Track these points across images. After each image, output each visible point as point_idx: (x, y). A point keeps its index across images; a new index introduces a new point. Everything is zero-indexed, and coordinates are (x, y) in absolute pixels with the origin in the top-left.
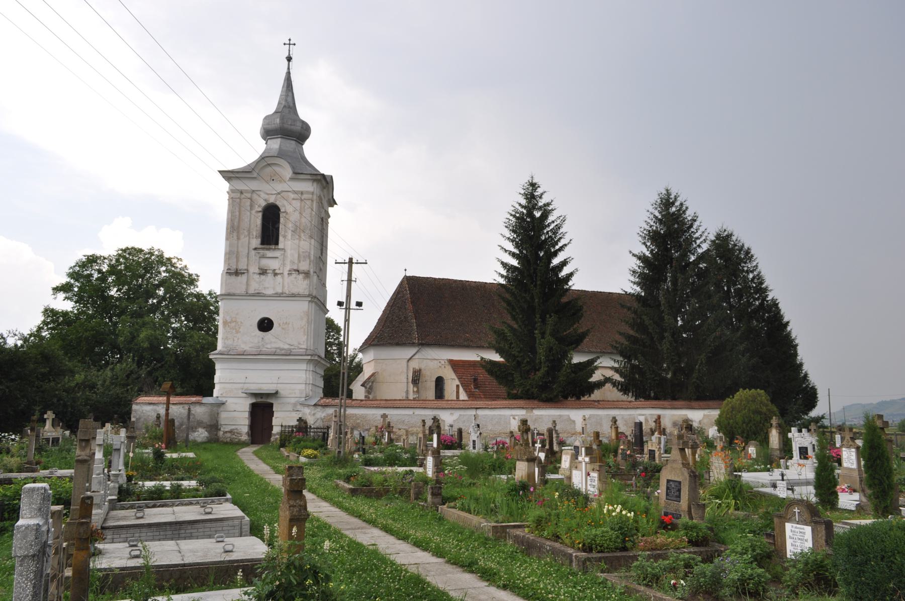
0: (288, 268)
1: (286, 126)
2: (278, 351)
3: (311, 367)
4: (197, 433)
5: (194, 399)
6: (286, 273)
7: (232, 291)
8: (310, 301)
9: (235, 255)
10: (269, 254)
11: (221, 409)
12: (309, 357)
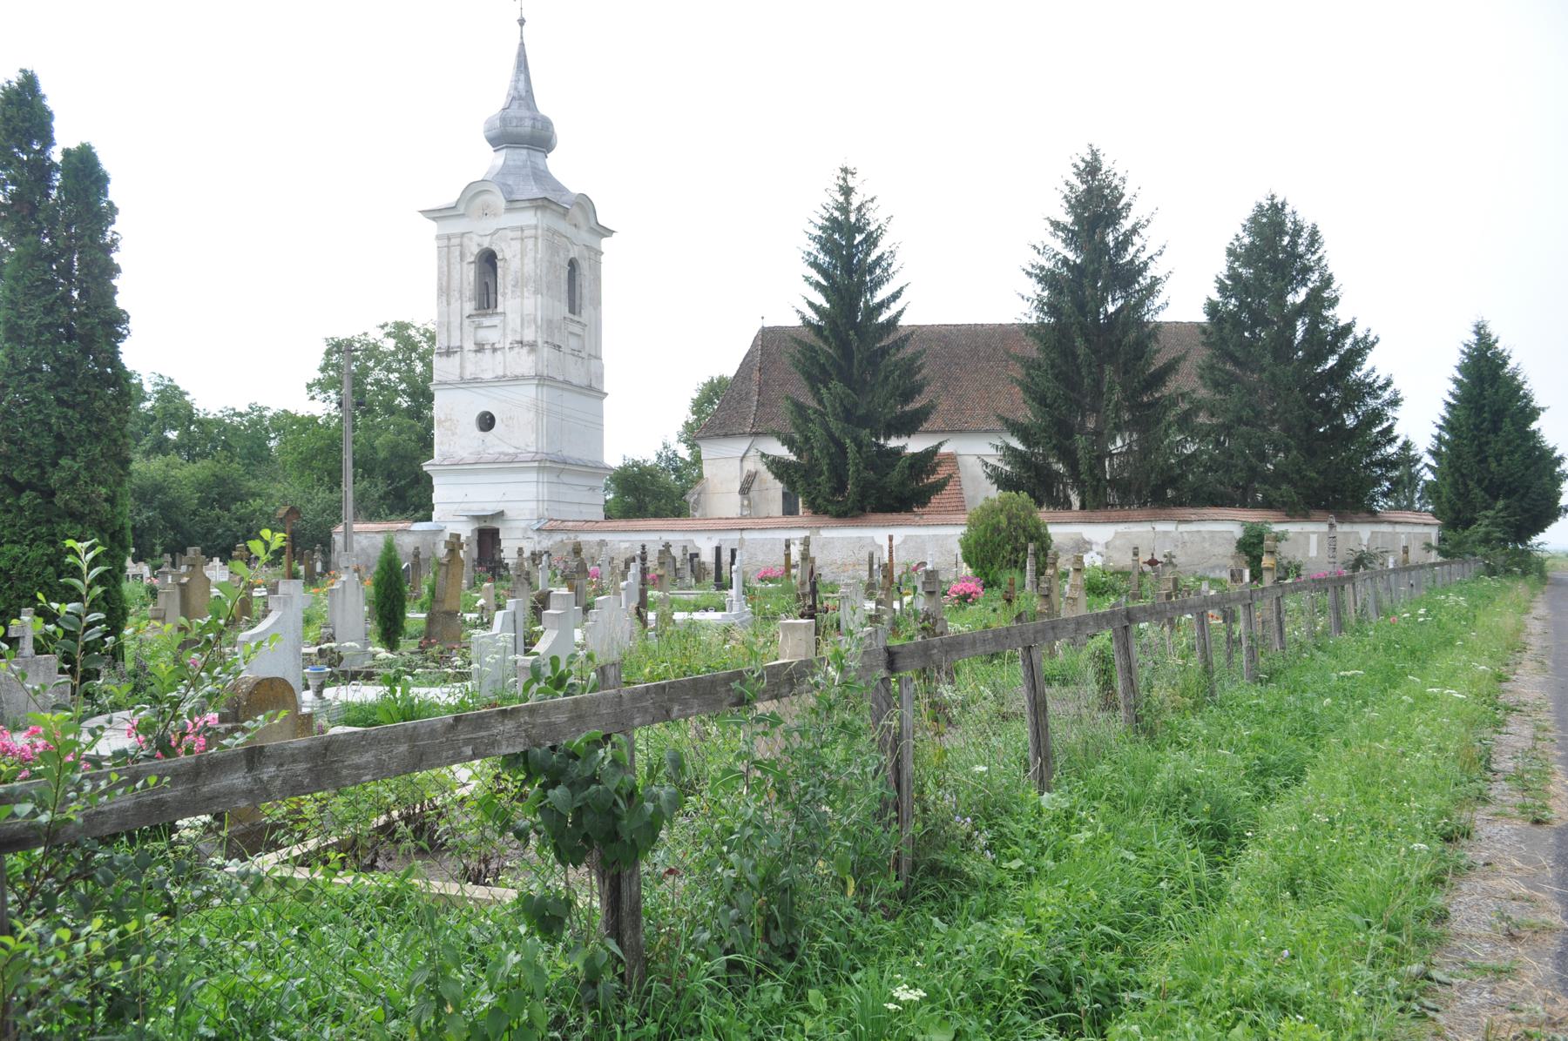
0: (510, 339)
1: (510, 129)
8: (537, 385)
10: (487, 321)
12: (536, 464)
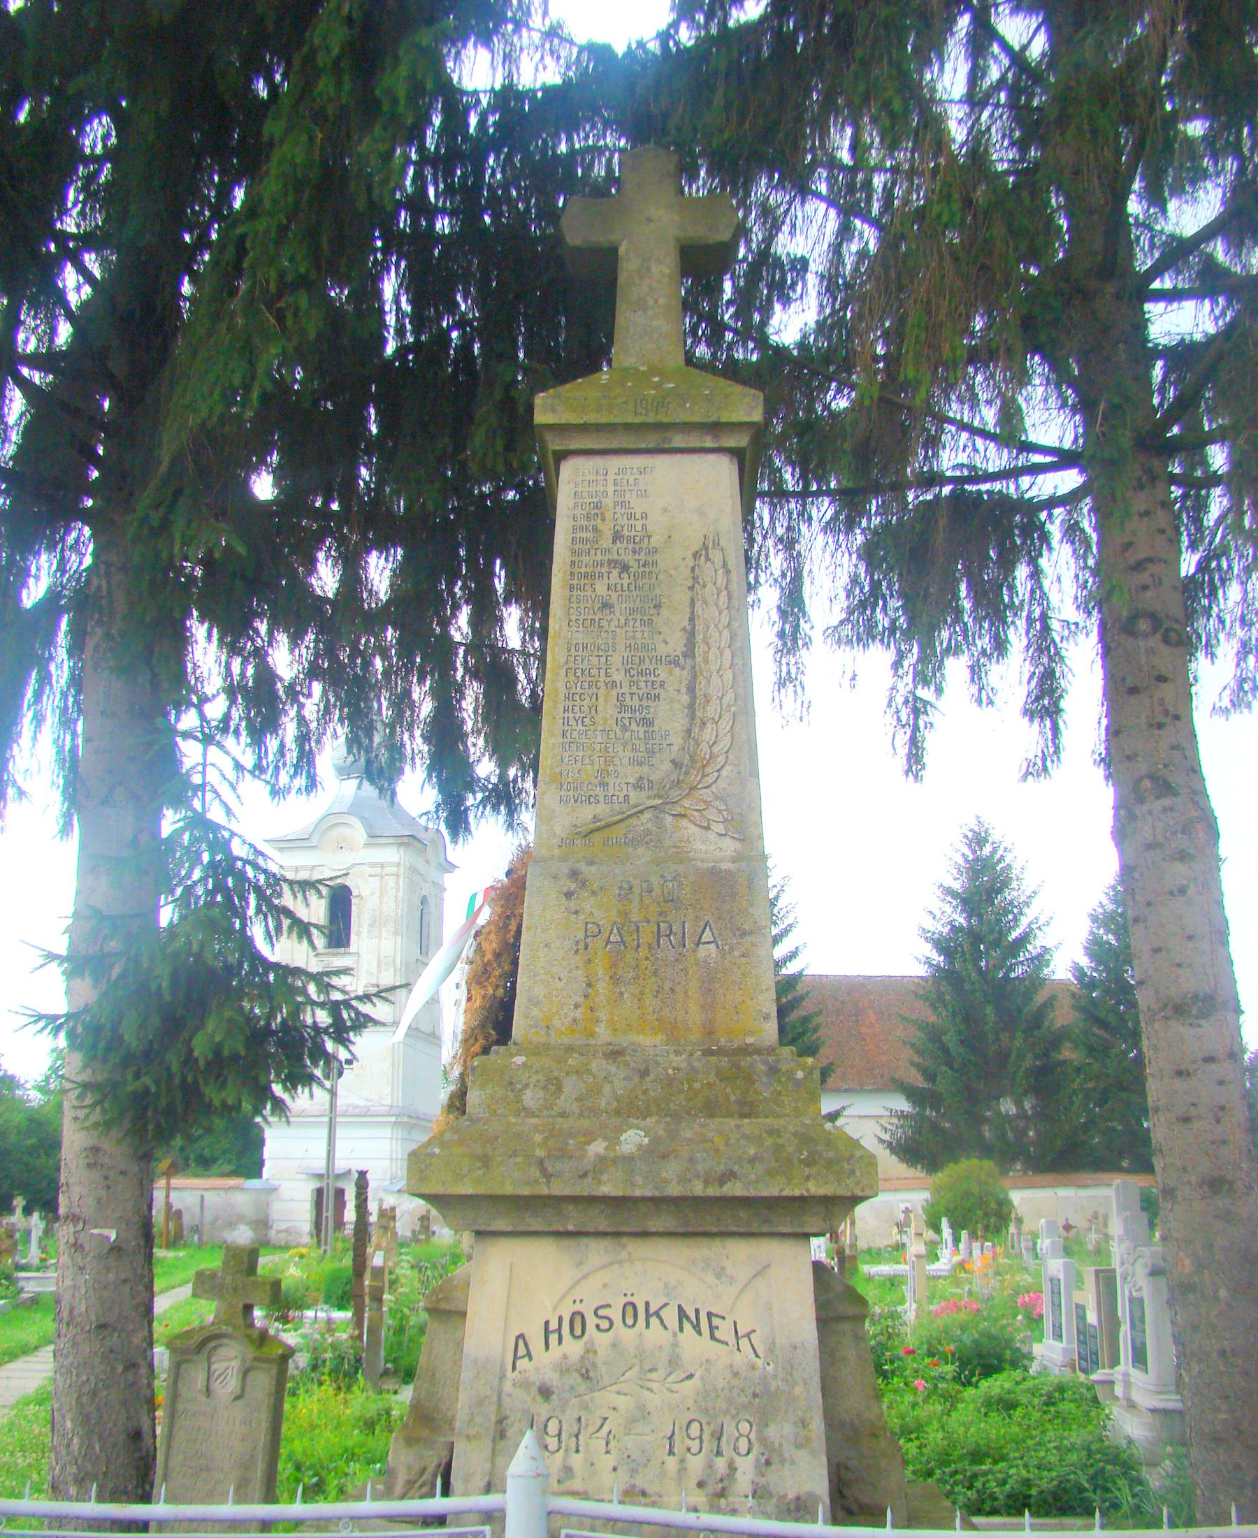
3: (399, 1133)
5: (232, 1182)
12: (394, 1119)
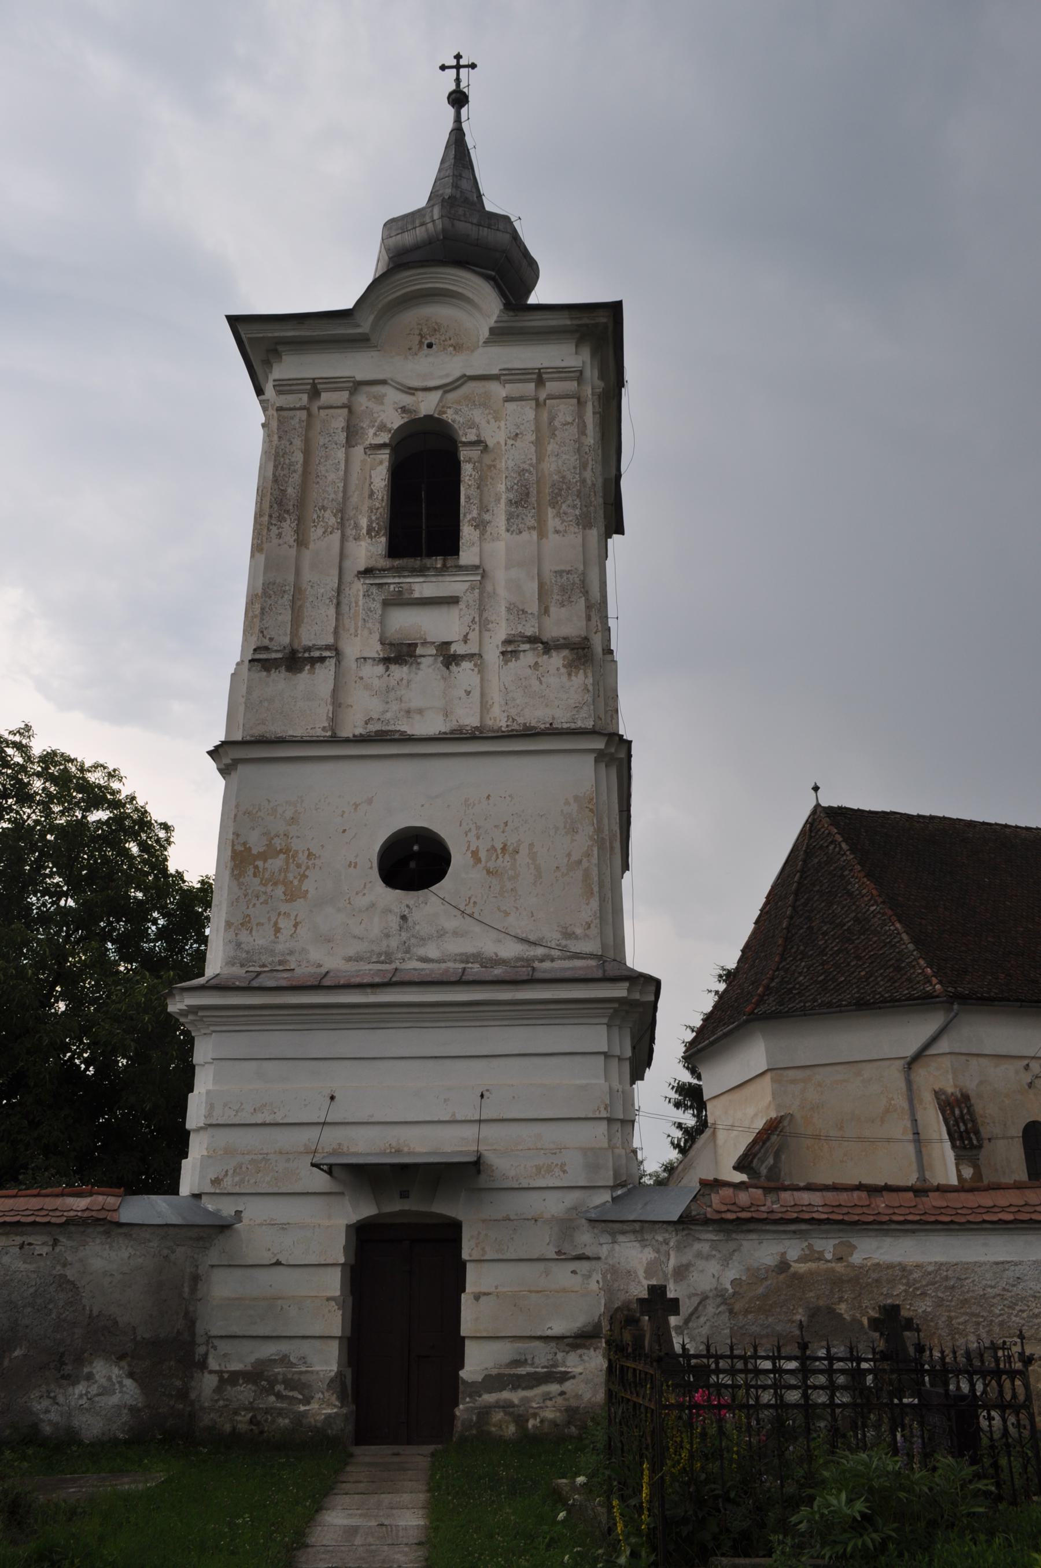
0: (500, 632)
2: (476, 967)
4: (80, 1388)
6: (492, 655)
7: (277, 729)
9: (288, 597)
10: (424, 587)
11: (213, 1256)
